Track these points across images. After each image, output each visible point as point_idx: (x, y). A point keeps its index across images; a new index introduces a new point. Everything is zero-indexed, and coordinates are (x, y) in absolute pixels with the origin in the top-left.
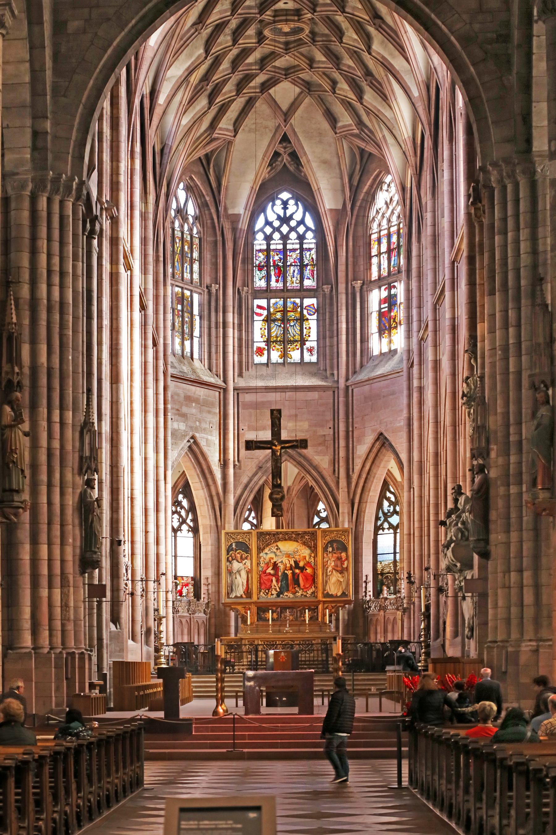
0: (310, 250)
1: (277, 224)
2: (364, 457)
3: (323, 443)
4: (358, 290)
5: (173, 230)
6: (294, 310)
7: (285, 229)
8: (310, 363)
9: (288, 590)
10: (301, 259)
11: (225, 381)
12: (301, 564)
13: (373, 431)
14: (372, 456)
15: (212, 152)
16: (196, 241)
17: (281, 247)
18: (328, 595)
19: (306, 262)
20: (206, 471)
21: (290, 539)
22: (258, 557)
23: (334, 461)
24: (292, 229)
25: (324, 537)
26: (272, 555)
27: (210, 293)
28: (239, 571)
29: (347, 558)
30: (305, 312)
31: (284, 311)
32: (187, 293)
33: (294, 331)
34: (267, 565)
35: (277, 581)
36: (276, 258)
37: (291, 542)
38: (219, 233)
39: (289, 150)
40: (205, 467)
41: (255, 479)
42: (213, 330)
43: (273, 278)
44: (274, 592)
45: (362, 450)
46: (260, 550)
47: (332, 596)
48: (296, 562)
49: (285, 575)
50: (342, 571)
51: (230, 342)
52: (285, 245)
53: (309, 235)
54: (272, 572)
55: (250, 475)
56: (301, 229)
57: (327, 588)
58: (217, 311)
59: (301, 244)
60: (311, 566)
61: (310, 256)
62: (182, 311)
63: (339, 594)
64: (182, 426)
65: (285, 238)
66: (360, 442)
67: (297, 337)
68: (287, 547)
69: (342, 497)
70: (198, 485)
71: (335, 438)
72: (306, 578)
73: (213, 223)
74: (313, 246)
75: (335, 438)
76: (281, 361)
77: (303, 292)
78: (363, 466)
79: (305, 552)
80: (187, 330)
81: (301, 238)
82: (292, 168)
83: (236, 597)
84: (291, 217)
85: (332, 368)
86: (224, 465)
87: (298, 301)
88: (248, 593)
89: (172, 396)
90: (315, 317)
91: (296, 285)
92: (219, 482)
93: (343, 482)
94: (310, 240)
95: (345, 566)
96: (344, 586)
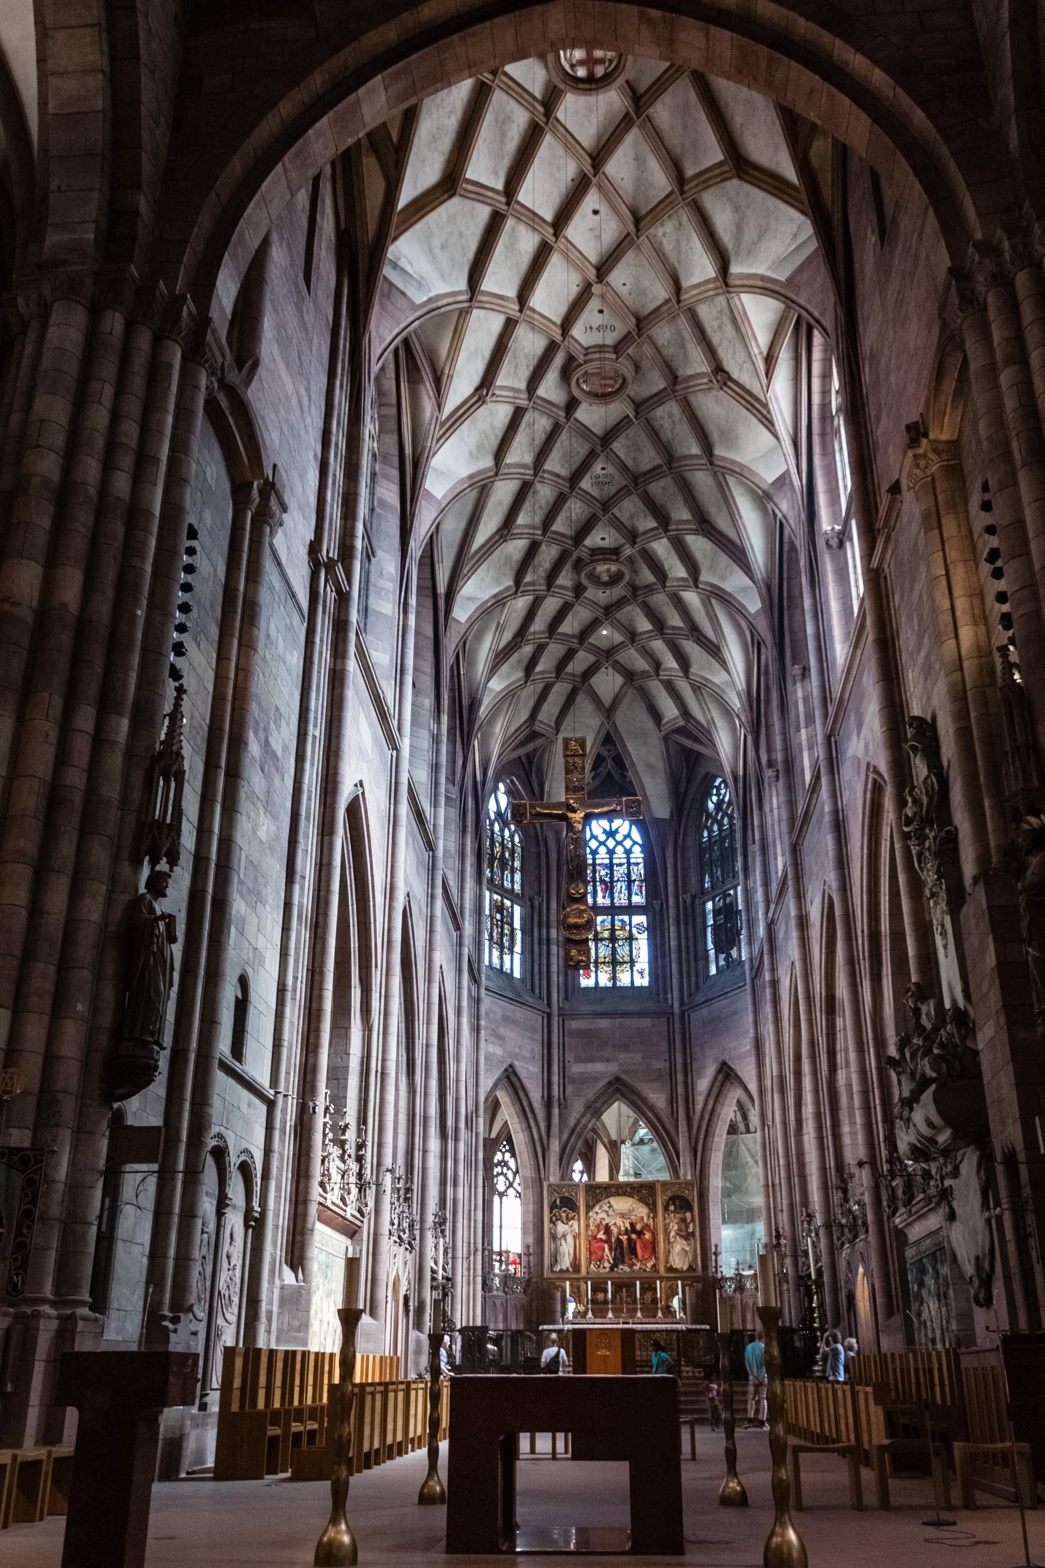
0: (637, 864)
1: (602, 837)
2: (706, 1092)
3: (659, 1078)
4: (689, 900)
5: (493, 832)
6: (623, 928)
7: (611, 843)
8: (641, 988)
9: (623, 1262)
10: (629, 875)
11: (549, 1005)
12: (638, 1227)
13: (715, 1060)
14: (715, 1090)
15: (535, 750)
16: (519, 850)
17: (607, 861)
18: (670, 1269)
19: (634, 877)
20: (527, 1109)
21: (624, 1194)
22: (588, 1218)
23: (672, 1100)
24: (618, 843)
25: (663, 1192)
26: (604, 1215)
27: (532, 907)
28: (564, 1236)
29: (693, 1220)
30: (634, 931)
31: (613, 930)
32: (508, 903)
33: (623, 951)
34: (598, 1227)
35: (610, 1249)
36: (603, 873)
37: (625, 1198)
38: (542, 844)
39: (613, 754)
40: (525, 1103)
41: (584, 1121)
42: (536, 947)
43: (600, 894)
44: (607, 1264)
45: (703, 1085)
46: (589, 1208)
47: (676, 1270)
48: (632, 1225)
49: (619, 1242)
50: (687, 1237)
51: (554, 960)
52: (611, 859)
53: (637, 851)
54: (604, 1237)
55: (578, 1116)
56: (628, 843)
57: (671, 1259)
58: (540, 927)
59: (628, 858)
60: (650, 1230)
61: (639, 871)
62: (502, 921)
63: (685, 1268)
64: (499, 1051)
65: (611, 852)
66: (700, 1075)
67: (627, 959)
68: (622, 1204)
69: (682, 1142)
70: (518, 1127)
71: (672, 1073)
72: (645, 1248)
73: (536, 833)
74: (640, 860)
75: (672, 1073)
76: (610, 984)
77: (631, 909)
78: (705, 1105)
79: (642, 1211)
80: (506, 944)
81: (628, 852)
82: (617, 776)
83: (561, 1271)
84: (617, 831)
85: (666, 993)
86: (548, 1104)
87: (626, 918)
88: (576, 1266)
89: (487, 1014)
90: (645, 935)
91: (624, 902)
92: (543, 1125)
93: (682, 1126)
94: (637, 854)
95: (691, 1229)
96: (690, 1256)
